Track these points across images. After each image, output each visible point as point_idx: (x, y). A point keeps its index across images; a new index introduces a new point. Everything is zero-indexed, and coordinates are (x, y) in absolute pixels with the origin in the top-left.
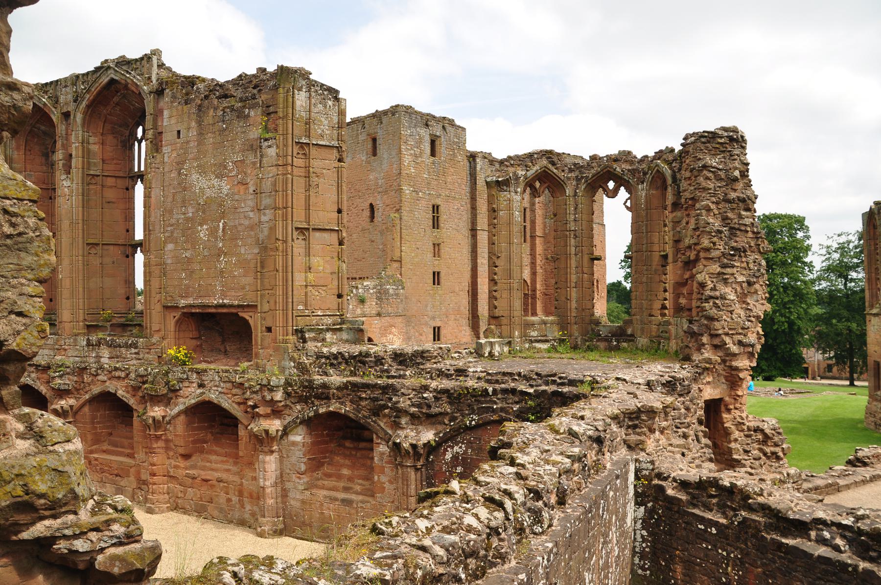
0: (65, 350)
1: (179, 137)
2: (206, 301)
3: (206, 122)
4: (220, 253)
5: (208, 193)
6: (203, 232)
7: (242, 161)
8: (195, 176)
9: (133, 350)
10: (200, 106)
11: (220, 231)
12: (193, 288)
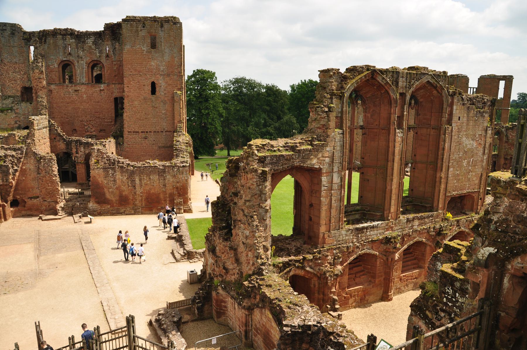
0: (392, 227)
1: (459, 120)
2: (460, 192)
3: (470, 116)
4: (470, 171)
5: (469, 146)
6: (465, 163)
7: (481, 135)
8: (464, 139)
9: (431, 218)
10: (469, 107)
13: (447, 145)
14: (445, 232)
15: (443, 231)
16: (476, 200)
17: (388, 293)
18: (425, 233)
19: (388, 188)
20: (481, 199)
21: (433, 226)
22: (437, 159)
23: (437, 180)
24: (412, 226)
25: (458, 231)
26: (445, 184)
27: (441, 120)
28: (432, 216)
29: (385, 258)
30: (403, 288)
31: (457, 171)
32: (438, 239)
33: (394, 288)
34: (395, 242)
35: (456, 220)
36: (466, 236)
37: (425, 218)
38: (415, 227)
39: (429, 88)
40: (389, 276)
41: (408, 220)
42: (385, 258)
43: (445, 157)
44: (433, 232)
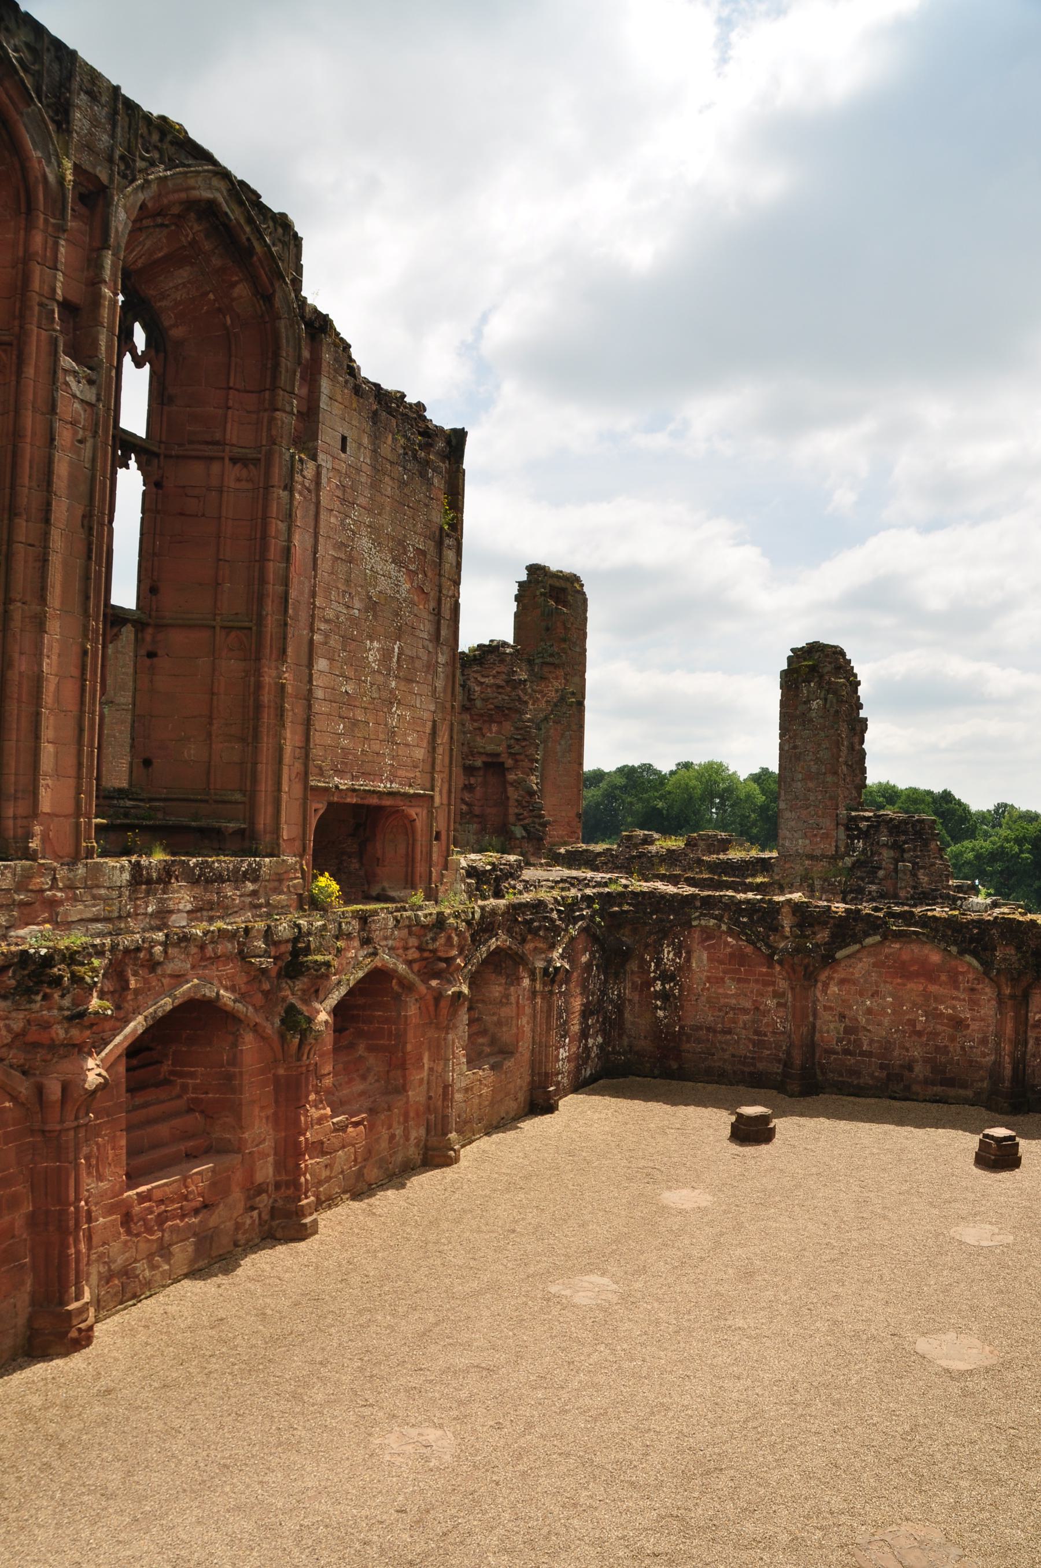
1: (344, 449)
2: (360, 784)
5: (383, 584)
9: (250, 886)
11: (395, 660)
12: (355, 755)
13: (300, 540)
14: (319, 958)
15: (307, 951)
16: (421, 839)
17: (63, 1303)
18: (228, 958)
19: (22, 665)
20: (438, 837)
21: (261, 925)
22: (261, 598)
23: (266, 698)
24: (163, 914)
25: (369, 964)
26: (300, 729)
27: (272, 420)
28: (253, 875)
29: (24, 1088)
30: (143, 1269)
31: (348, 679)
32: (291, 993)
33: (95, 1271)
34: (76, 979)
35: (356, 915)
36: (397, 997)
37: (220, 879)
38: (179, 921)
39: (216, 262)
40: (62, 1201)
41: (139, 877)
42: (24, 1088)
43: (293, 594)
44: (266, 954)
